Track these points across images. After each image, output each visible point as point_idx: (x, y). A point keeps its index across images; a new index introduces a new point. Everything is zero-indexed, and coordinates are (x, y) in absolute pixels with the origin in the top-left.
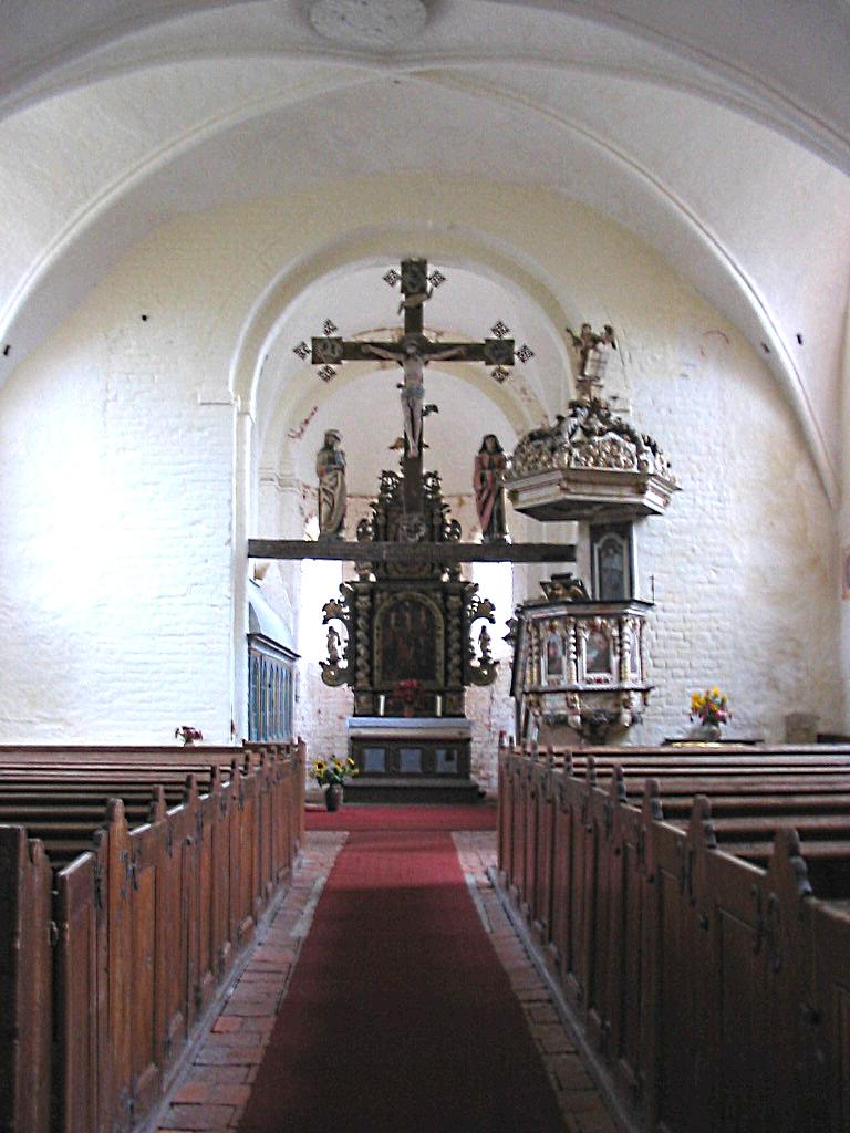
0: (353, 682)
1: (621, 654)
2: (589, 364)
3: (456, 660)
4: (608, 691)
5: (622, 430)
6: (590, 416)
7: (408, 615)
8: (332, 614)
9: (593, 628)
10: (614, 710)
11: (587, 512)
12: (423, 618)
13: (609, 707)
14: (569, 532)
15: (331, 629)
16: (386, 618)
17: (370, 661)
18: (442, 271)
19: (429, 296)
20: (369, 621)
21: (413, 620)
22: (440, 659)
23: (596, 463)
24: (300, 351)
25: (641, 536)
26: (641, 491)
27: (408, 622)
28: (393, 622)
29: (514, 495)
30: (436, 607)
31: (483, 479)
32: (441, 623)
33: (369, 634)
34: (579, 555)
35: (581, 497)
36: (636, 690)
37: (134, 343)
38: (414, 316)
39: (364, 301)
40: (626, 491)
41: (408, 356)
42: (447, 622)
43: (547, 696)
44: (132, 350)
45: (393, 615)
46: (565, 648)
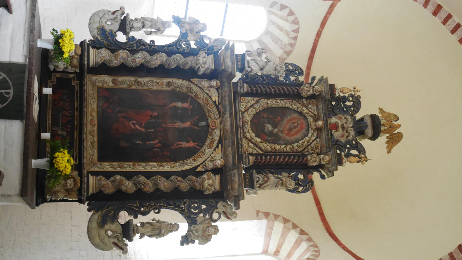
7: (188, 124)
8: (187, 27)
12: (184, 144)
15: (165, 25)
16: (182, 96)
21: (181, 131)
22: (129, 167)
27: (180, 125)
28: (179, 104)
30: (200, 161)
32: (177, 167)
42: (184, 174)
45: (186, 105)
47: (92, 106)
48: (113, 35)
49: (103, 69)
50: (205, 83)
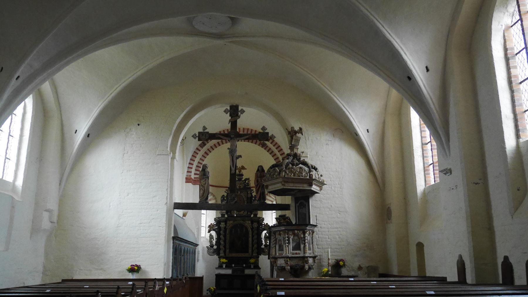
0: (218, 254)
1: (305, 244)
2: (293, 141)
3: (255, 246)
4: (299, 257)
5: (305, 164)
6: (293, 159)
9: (294, 234)
10: (302, 265)
11: (292, 192)
12: (244, 230)
13: (300, 263)
14: (287, 200)
15: (211, 235)
17: (225, 247)
18: (244, 109)
19: (239, 117)
20: (225, 232)
22: (250, 246)
23: (294, 175)
24: (194, 136)
25: (312, 202)
26: (311, 185)
29: (267, 187)
31: (257, 181)
32: (250, 233)
33: (225, 236)
34: (291, 208)
35: (289, 187)
36: (310, 257)
37: (135, 133)
38: (234, 124)
39: (216, 119)
40: (305, 185)
41: (231, 138)
42: (253, 232)
43: (279, 259)
44: (133, 136)
46: (284, 241)
47: (234, 255)
48: (214, 249)
49: (225, 252)
50: (228, 225)
